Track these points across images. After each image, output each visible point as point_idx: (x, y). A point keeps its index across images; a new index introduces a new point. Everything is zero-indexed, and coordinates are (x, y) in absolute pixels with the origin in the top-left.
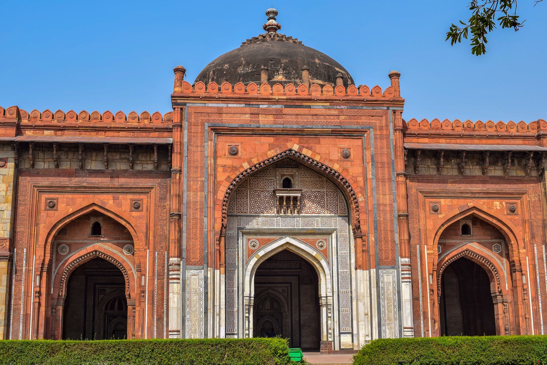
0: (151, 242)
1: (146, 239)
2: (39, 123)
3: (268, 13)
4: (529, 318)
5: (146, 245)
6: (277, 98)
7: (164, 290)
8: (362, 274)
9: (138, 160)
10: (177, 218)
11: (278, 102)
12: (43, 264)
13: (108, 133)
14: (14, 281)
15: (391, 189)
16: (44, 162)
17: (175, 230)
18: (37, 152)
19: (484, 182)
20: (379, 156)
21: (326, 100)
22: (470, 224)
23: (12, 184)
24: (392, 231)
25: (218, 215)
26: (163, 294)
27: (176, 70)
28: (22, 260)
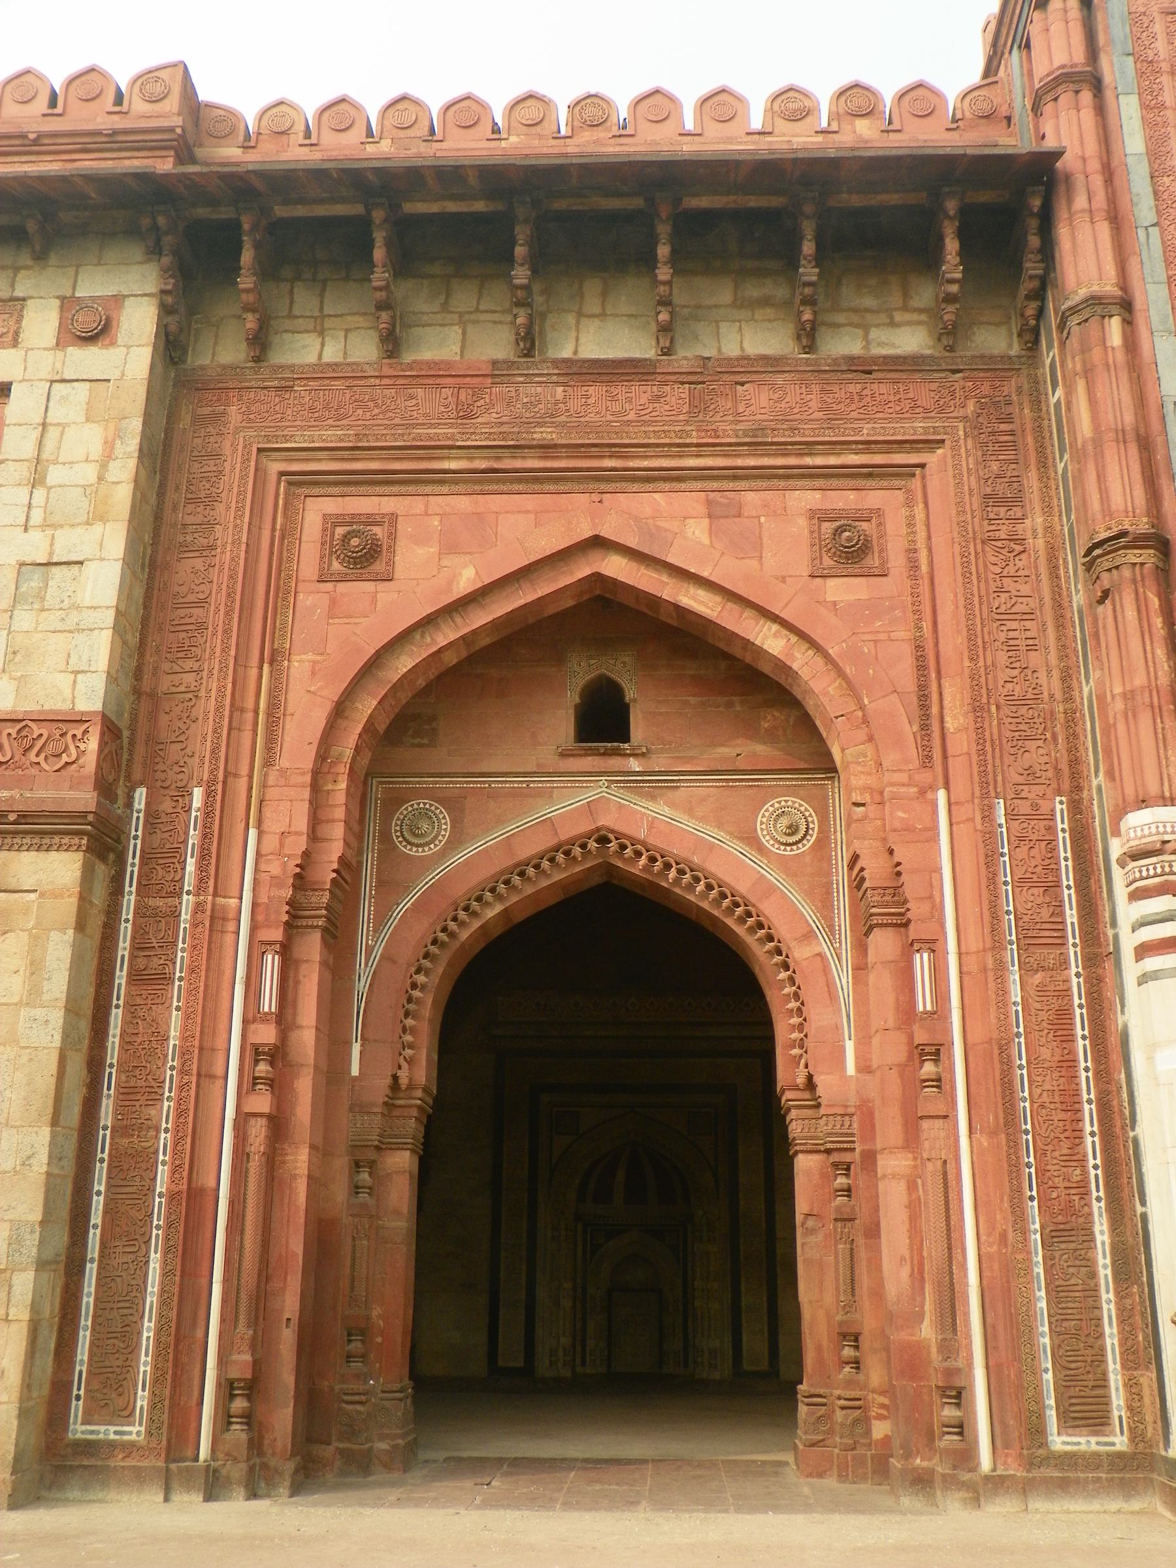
0: (961, 743)
1: (925, 727)
5: (926, 760)
7: (1071, 1038)
9: (836, 308)
10: (1148, 557)
12: (301, 881)
14: (121, 977)
16: (321, 333)
17: (1145, 629)
18: (285, 287)
23: (136, 424)
26: (1069, 1064)
28: (177, 854)
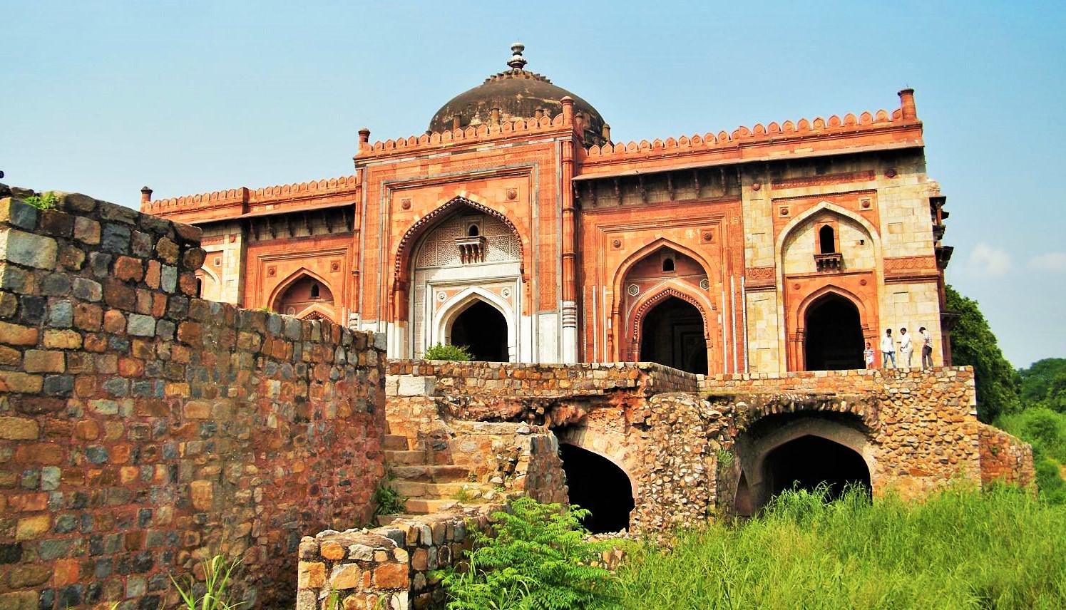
2: (262, 200)
3: (513, 49)
4: (723, 364)
6: (444, 145)
8: (526, 320)
11: (445, 150)
13: (314, 202)
15: (554, 227)
19: (673, 207)
20: (543, 192)
21: (491, 141)
22: (674, 259)
24: (554, 273)
25: (392, 269)
27: (360, 133)
